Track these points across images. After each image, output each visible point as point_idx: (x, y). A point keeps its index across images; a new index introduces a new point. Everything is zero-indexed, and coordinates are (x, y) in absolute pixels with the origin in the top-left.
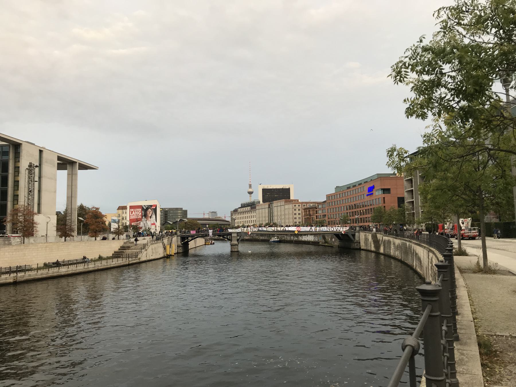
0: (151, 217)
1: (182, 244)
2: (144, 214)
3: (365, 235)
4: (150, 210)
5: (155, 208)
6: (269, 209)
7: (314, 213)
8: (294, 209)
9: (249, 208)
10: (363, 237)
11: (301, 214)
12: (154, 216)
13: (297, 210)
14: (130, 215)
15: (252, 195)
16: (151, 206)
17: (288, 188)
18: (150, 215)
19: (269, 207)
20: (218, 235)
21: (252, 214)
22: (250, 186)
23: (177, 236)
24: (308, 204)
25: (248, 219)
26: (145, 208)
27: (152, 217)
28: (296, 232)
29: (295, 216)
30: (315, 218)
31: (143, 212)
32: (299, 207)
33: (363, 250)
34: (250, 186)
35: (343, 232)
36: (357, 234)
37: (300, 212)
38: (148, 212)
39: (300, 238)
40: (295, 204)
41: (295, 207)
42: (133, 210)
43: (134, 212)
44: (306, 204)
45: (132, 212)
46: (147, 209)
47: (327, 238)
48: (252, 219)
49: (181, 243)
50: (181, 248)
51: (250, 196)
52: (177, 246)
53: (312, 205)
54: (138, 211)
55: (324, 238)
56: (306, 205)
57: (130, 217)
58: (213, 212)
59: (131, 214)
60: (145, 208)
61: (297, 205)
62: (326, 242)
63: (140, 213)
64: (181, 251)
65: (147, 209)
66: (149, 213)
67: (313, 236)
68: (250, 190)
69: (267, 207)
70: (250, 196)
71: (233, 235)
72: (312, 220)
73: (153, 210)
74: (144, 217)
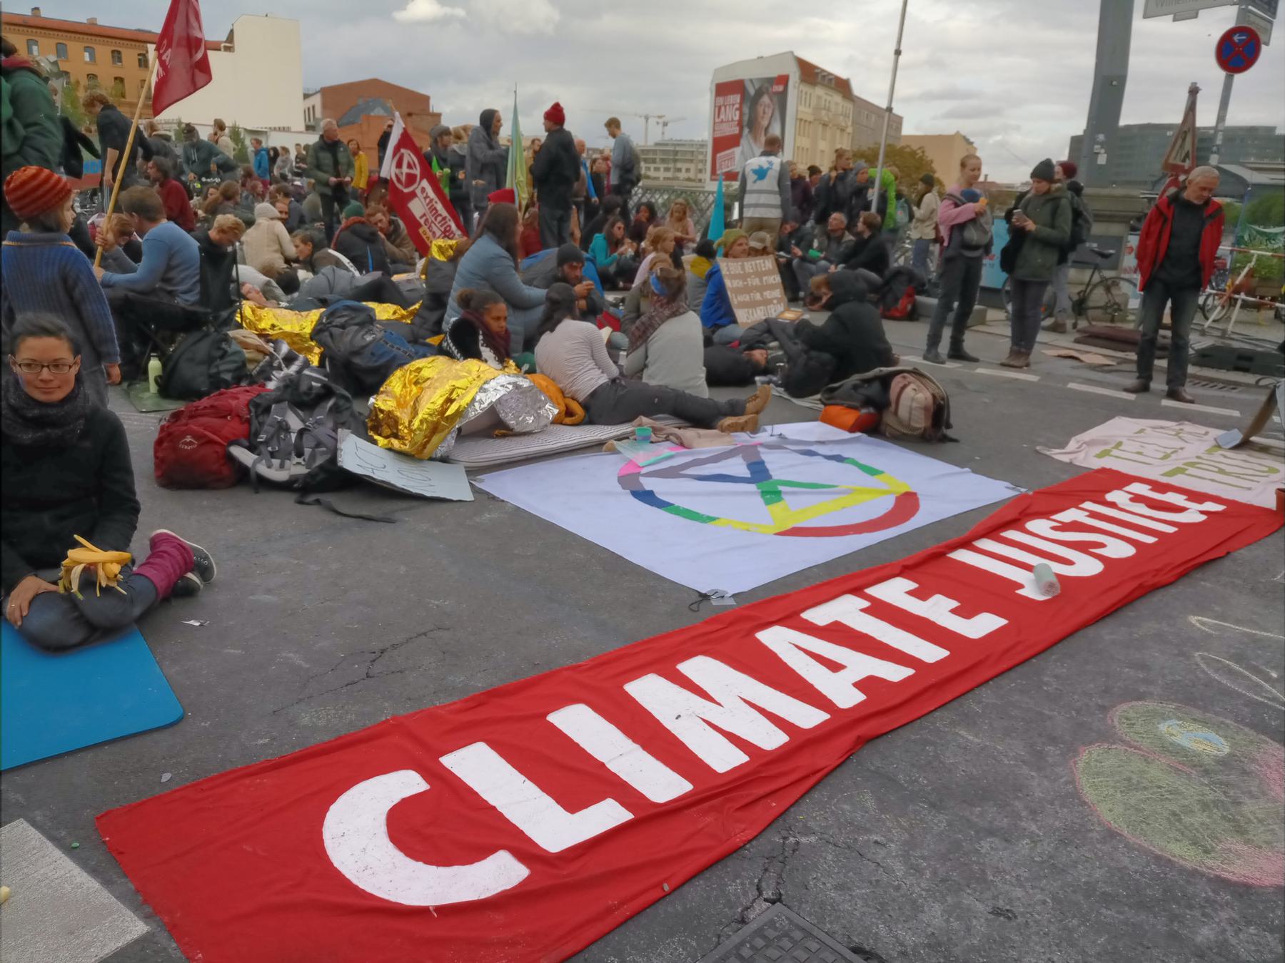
2: (746, 118)
5: (781, 88)
16: (772, 81)
18: (765, 123)
26: (752, 91)
31: (746, 110)
38: (760, 110)
42: (721, 100)
43: (723, 108)
46: (759, 93)
54: (733, 105)
57: (714, 130)
59: (717, 120)
60: (752, 91)
63: (738, 113)
65: (759, 93)
66: (764, 113)
73: (775, 99)
74: (746, 131)
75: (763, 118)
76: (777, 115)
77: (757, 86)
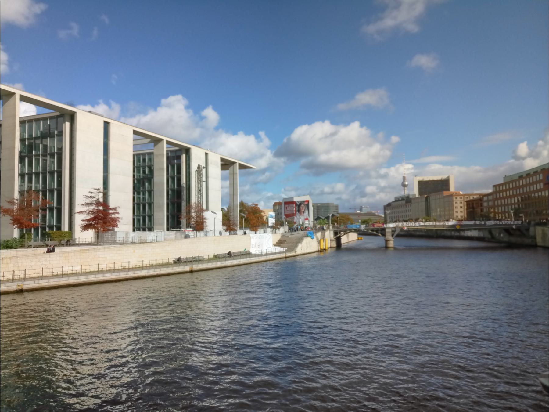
0: (304, 212)
1: (335, 239)
2: (297, 210)
3: (543, 231)
4: (303, 205)
5: (307, 203)
10: (540, 232)
11: (463, 207)
12: (307, 212)
13: (459, 202)
14: (285, 211)
16: (304, 201)
18: (303, 211)
21: (407, 209)
23: (330, 231)
25: (403, 214)
26: (298, 204)
27: (305, 212)
28: (458, 227)
31: (297, 208)
33: (540, 246)
35: (514, 227)
36: (532, 229)
37: (462, 205)
38: (301, 208)
39: (462, 234)
41: (456, 200)
42: (287, 206)
43: (288, 208)
45: (287, 208)
46: (300, 204)
47: (494, 233)
48: (408, 214)
52: (331, 241)
53: (475, 197)
55: (490, 232)
60: (298, 204)
62: (493, 237)
67: (477, 231)
71: (387, 230)
73: (306, 205)
74: (297, 212)
75: (302, 209)
76: (307, 209)
77: (300, 202)
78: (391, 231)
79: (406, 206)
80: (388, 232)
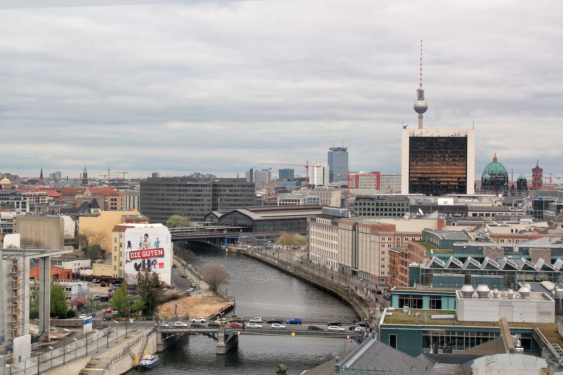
1: (163, 341)
6: (354, 232)
7: (398, 262)
8: (381, 244)
9: (329, 222)
15: (424, 114)
17: (462, 135)
19: (354, 229)
20: (203, 334)
22: (421, 95)
23: (157, 333)
24: (404, 238)
29: (382, 256)
30: (399, 271)
32: (390, 241)
34: (421, 95)
40: (383, 237)
44: (400, 238)
49: (162, 340)
50: (161, 346)
51: (421, 118)
52: (157, 345)
56: (402, 239)
58: (338, 149)
61: (386, 238)
64: (161, 350)
68: (421, 104)
69: (351, 229)
70: (421, 118)
72: (396, 271)
78: (223, 335)
79: (332, 229)
80: (221, 337)
